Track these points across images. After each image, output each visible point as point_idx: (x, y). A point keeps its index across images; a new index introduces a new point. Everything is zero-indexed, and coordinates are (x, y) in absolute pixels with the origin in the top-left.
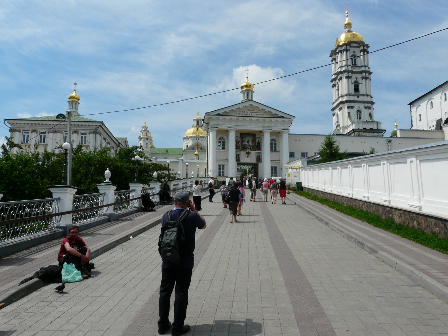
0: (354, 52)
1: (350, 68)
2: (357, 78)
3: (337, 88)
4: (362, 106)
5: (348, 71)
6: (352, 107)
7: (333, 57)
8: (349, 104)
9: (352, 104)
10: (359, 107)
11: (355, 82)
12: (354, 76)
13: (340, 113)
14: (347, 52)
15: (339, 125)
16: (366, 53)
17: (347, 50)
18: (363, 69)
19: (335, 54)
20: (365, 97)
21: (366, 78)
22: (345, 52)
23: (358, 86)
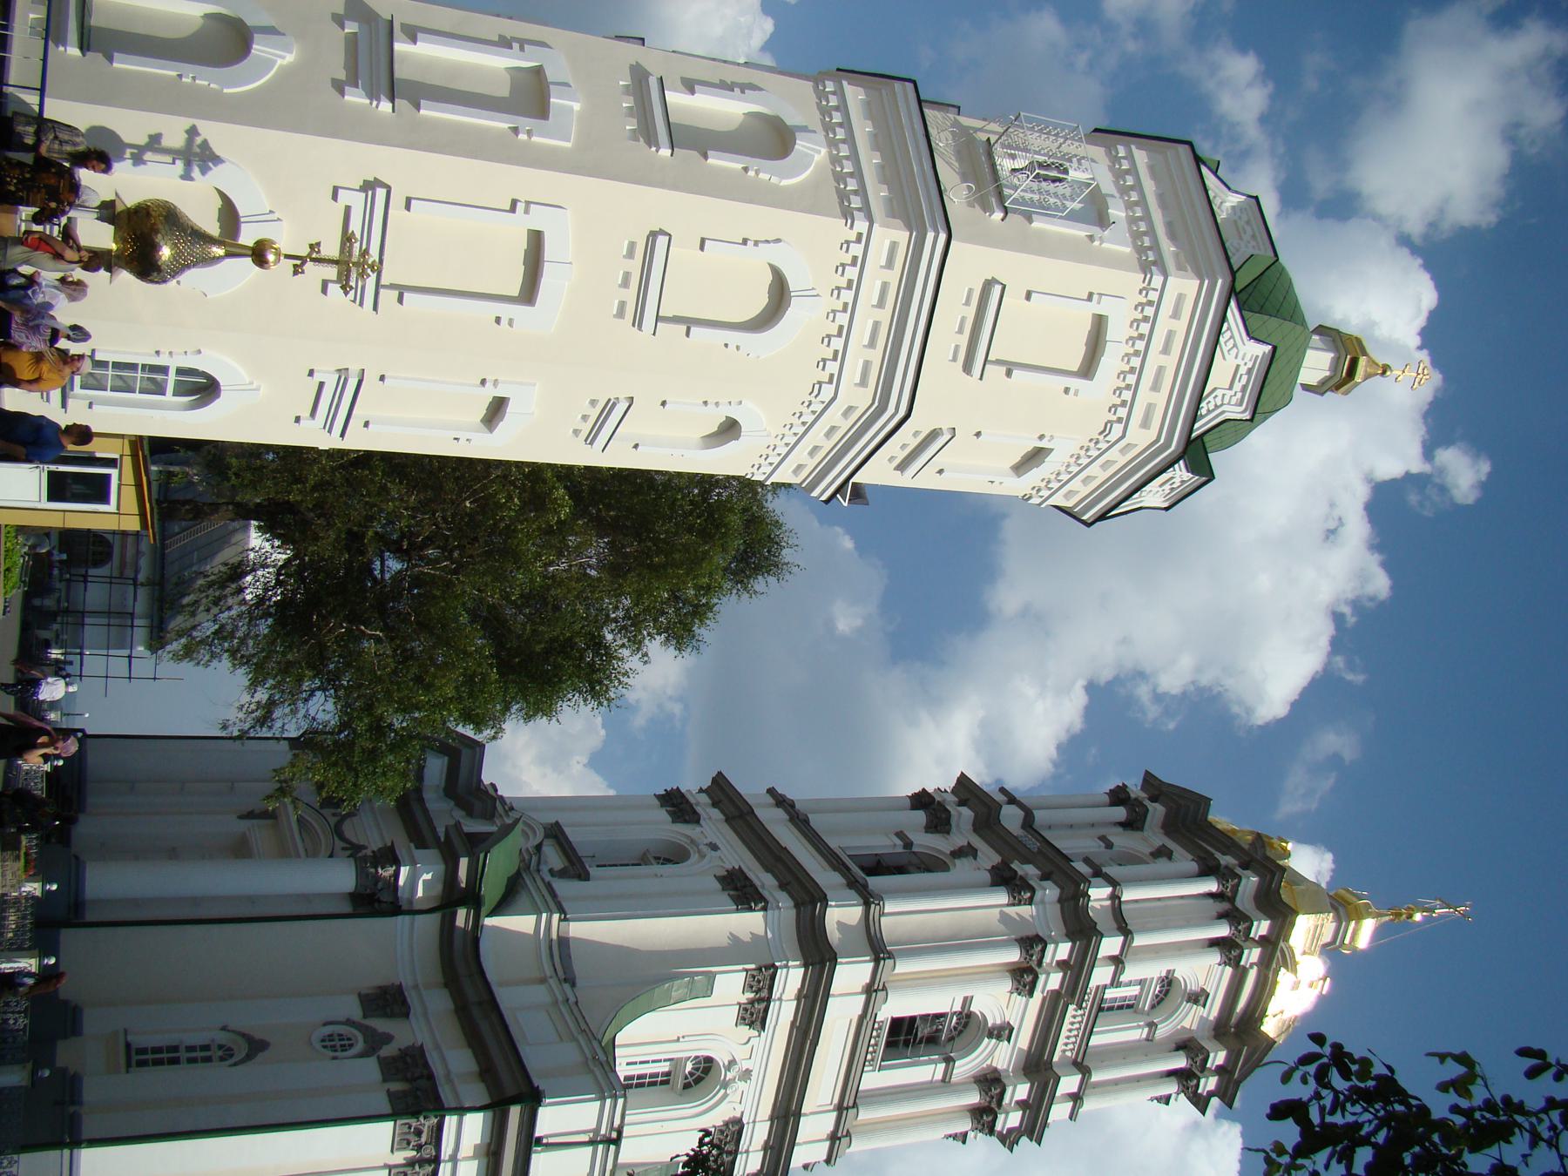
0: (1198, 998)
1: (1101, 975)
2: (1003, 1032)
3: (926, 842)
4: (749, 1101)
5: (1076, 970)
6: (754, 1015)
7: (1157, 811)
8: (791, 979)
9: (783, 1012)
10: (746, 1075)
11: (966, 1019)
12: (1024, 1013)
13: (701, 873)
14: (1214, 943)
15: (584, 876)
16: (1171, 1088)
17: (1228, 948)
18: (1069, 1083)
19: (1171, 827)
20: (828, 1122)
21: (984, 1117)
22: (1223, 931)
23: (932, 1040)
